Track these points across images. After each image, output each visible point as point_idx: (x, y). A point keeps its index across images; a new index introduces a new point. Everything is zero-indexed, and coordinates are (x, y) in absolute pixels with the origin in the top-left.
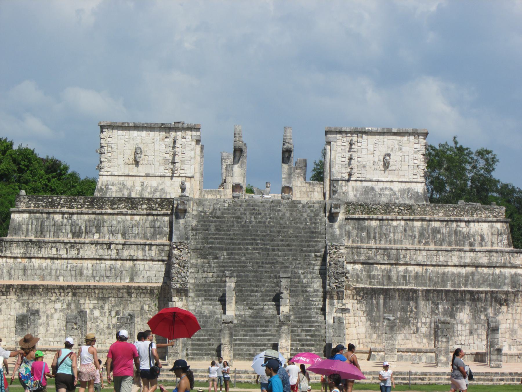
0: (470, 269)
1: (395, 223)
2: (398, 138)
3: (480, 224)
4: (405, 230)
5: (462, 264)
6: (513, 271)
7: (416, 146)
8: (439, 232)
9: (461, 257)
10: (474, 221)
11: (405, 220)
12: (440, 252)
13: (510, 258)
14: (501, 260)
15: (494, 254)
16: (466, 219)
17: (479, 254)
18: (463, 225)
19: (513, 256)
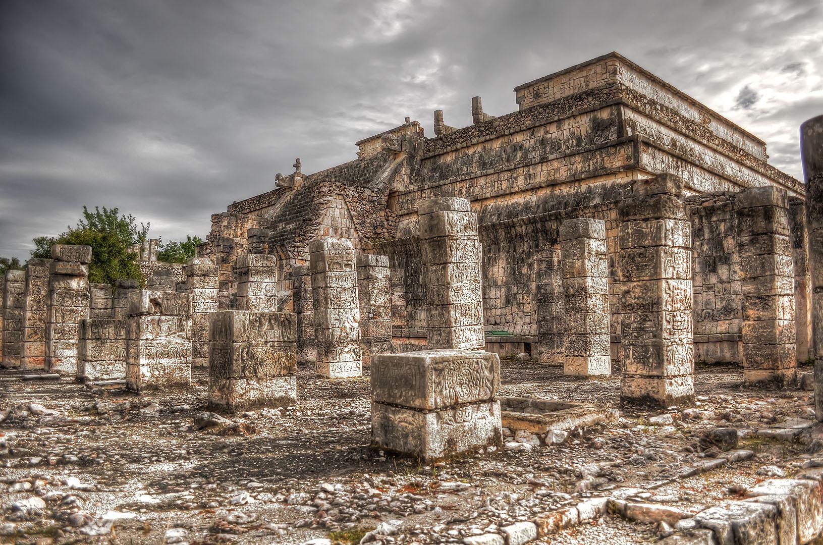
0: (542, 193)
1: (471, 151)
2: (584, 74)
3: (578, 119)
4: (481, 157)
5: (530, 186)
6: (609, 182)
7: (604, 76)
8: (521, 148)
9: (530, 175)
10: (568, 118)
11: (482, 143)
12: (502, 175)
13: (603, 160)
14: (589, 166)
15: (578, 159)
16: (556, 118)
17: (556, 164)
18: (553, 128)
19: (609, 155)
